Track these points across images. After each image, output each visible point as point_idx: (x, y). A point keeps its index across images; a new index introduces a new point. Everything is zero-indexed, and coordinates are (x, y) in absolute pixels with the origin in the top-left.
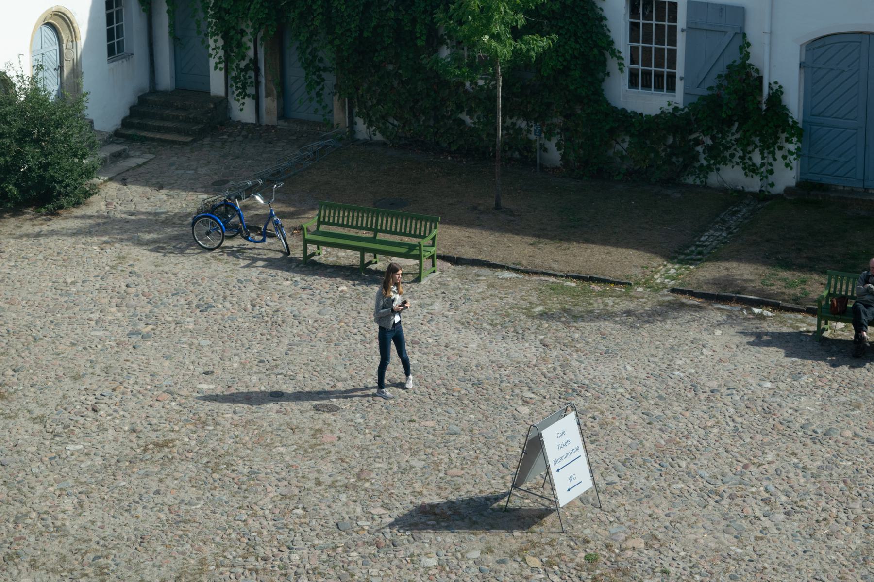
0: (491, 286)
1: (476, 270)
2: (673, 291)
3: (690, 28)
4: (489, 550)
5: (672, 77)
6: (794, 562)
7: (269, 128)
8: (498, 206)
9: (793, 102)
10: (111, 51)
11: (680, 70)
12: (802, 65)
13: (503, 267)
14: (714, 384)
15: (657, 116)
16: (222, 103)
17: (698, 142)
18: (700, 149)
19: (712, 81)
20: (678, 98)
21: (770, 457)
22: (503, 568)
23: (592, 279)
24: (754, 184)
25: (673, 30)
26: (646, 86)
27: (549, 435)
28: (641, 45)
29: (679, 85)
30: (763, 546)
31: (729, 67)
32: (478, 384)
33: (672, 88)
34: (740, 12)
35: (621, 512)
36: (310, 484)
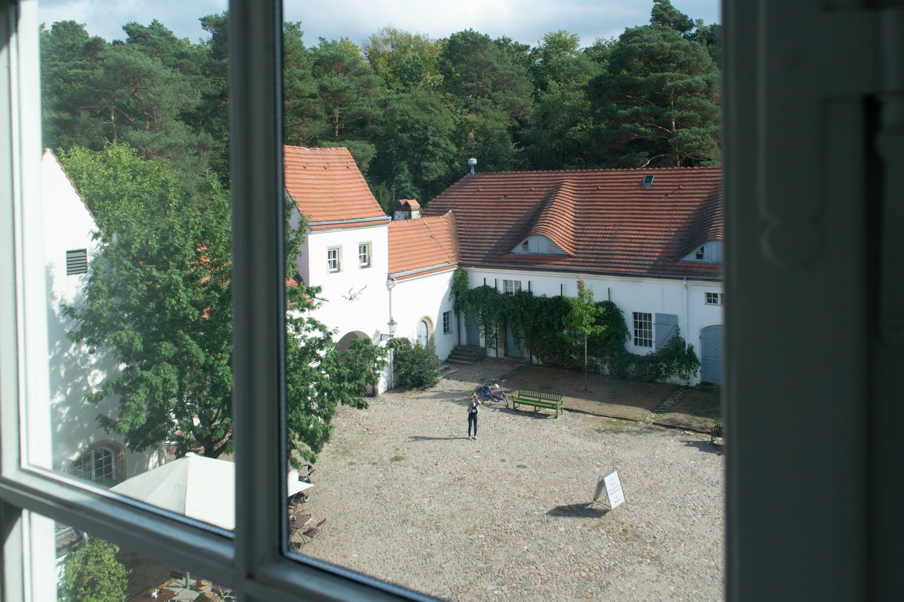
0: (584, 420)
1: (578, 414)
2: (654, 424)
3: (657, 323)
4: (585, 525)
5: (650, 341)
6: (706, 535)
7: (501, 359)
8: (586, 390)
9: (698, 351)
10: (445, 331)
11: (653, 339)
12: (700, 337)
13: (588, 413)
14: (671, 461)
15: (645, 356)
16: (484, 350)
17: (661, 366)
18: (662, 369)
19: (666, 343)
20: (653, 349)
21: (695, 491)
22: (590, 533)
23: (622, 419)
24: (683, 383)
25: (650, 324)
26: (641, 344)
27: (607, 480)
28: (638, 329)
29: (654, 344)
30: (694, 528)
31: (672, 338)
32: (579, 459)
33: (651, 345)
34: (675, 317)
35: (636, 512)
36: (516, 496)
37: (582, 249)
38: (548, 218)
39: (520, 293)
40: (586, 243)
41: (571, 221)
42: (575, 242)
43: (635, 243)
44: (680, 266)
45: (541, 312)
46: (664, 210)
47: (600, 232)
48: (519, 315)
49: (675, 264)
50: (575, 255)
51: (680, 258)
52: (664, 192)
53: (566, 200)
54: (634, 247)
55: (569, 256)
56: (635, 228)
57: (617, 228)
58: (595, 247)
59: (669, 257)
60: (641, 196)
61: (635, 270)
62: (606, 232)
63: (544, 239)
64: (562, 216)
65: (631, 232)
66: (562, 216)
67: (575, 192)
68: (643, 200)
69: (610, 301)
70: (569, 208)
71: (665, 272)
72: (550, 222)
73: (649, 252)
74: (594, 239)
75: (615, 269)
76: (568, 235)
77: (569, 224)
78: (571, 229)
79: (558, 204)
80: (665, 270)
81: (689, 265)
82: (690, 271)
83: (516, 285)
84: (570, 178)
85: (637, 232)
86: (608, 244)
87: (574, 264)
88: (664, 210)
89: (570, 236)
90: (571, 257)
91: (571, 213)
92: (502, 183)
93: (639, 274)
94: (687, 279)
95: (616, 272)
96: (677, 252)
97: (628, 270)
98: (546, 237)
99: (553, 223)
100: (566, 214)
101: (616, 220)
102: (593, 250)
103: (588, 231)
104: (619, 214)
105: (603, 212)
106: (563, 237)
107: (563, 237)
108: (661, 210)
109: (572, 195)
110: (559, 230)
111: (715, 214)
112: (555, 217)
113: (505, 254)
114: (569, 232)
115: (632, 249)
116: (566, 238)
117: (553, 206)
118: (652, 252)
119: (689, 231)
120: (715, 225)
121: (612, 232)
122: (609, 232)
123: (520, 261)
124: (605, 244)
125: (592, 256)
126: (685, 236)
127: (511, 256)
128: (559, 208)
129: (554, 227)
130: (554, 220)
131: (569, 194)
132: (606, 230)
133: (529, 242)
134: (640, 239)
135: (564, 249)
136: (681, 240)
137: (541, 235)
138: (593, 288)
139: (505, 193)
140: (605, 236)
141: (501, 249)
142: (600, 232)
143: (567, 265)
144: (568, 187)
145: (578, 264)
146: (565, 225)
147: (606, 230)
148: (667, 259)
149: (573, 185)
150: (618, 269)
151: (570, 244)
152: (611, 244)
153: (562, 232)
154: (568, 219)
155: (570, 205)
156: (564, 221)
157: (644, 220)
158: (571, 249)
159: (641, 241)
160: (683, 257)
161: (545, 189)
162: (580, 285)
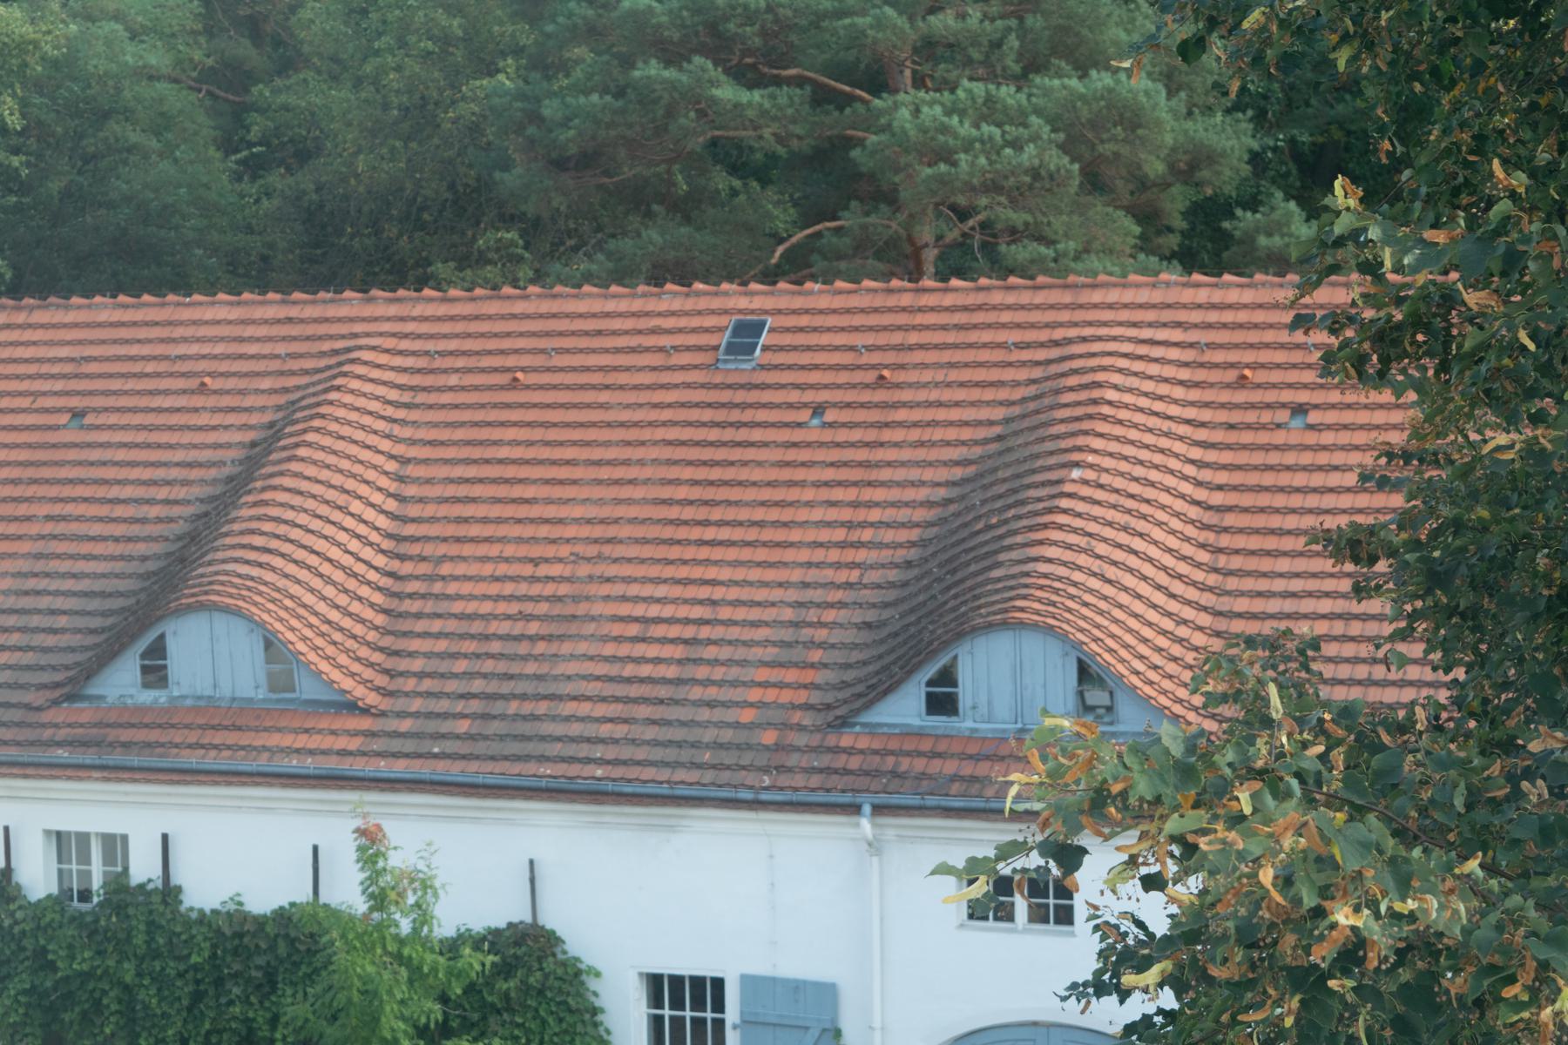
37: (421, 675)
38: (268, 527)
39: (120, 891)
40: (441, 646)
41: (375, 537)
42: (387, 641)
43: (664, 641)
44: (850, 751)
45: (219, 982)
46: (801, 484)
47: (508, 588)
48: (111, 1002)
49: (831, 740)
50: (385, 704)
51: (857, 712)
52: (809, 397)
53: (359, 435)
54: (657, 661)
55: (352, 707)
56: (669, 572)
57: (583, 570)
58: (476, 666)
59: (807, 707)
60: (707, 415)
61: (650, 772)
62: (536, 589)
63: (239, 626)
64: (337, 516)
65: (647, 590)
66: (337, 516)
67: (406, 397)
68: (714, 435)
69: (535, 925)
70: (371, 475)
71: (784, 780)
72: (274, 544)
73: (720, 684)
74: (477, 627)
75: (561, 769)
76: (355, 607)
77: (367, 553)
78: (372, 576)
79: (320, 455)
80: (782, 769)
81: (893, 745)
82: (895, 774)
83: (109, 858)
84: (386, 327)
85: (677, 591)
86: (540, 647)
87: (377, 745)
88: (801, 484)
89: (368, 614)
90: (366, 711)
91: (377, 498)
92: (64, 352)
93: (664, 790)
94: (878, 810)
95: (562, 784)
96: (845, 685)
97: (618, 772)
98: (249, 618)
99: (287, 548)
100: (356, 506)
101: (585, 531)
102: (470, 675)
103: (452, 588)
104: (601, 502)
105: (529, 492)
106: (334, 616)
107: (334, 616)
108: (792, 484)
109: (390, 411)
110: (317, 583)
111: (1022, 503)
112: (303, 519)
113: (56, 703)
114: (365, 591)
115: (646, 670)
116: (347, 623)
117: (295, 467)
118: (735, 684)
119: (905, 584)
120: (1014, 555)
121: (563, 589)
122: (549, 589)
123: (126, 735)
124: (523, 648)
125: (460, 706)
126: (886, 605)
127: (82, 712)
128: (325, 475)
129: (291, 569)
130: (295, 534)
131: (374, 406)
132: (534, 579)
133: (172, 645)
134: (687, 621)
135: (336, 675)
136: (868, 625)
137: (236, 612)
138: (435, 861)
139: (75, 402)
140: (529, 608)
141: (46, 677)
142: (508, 588)
143: (343, 753)
144: (376, 374)
145: (396, 745)
146: (347, 560)
147: (534, 579)
148: (797, 717)
149: (398, 361)
150: (574, 770)
151: (364, 652)
152: (553, 648)
153: (329, 591)
154: (362, 530)
155: (379, 460)
156: (342, 537)
157: (710, 534)
158: (368, 674)
159: (689, 632)
160: (868, 706)
161: (266, 384)
162: (370, 844)
